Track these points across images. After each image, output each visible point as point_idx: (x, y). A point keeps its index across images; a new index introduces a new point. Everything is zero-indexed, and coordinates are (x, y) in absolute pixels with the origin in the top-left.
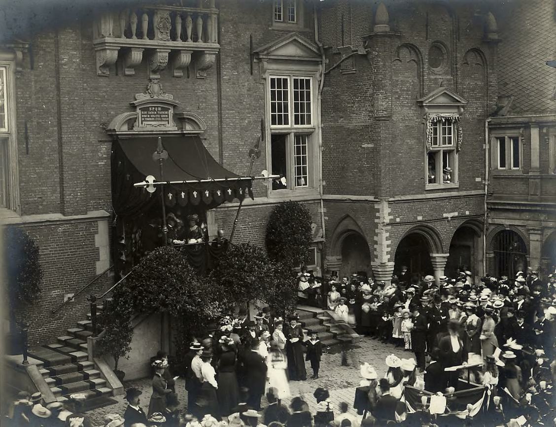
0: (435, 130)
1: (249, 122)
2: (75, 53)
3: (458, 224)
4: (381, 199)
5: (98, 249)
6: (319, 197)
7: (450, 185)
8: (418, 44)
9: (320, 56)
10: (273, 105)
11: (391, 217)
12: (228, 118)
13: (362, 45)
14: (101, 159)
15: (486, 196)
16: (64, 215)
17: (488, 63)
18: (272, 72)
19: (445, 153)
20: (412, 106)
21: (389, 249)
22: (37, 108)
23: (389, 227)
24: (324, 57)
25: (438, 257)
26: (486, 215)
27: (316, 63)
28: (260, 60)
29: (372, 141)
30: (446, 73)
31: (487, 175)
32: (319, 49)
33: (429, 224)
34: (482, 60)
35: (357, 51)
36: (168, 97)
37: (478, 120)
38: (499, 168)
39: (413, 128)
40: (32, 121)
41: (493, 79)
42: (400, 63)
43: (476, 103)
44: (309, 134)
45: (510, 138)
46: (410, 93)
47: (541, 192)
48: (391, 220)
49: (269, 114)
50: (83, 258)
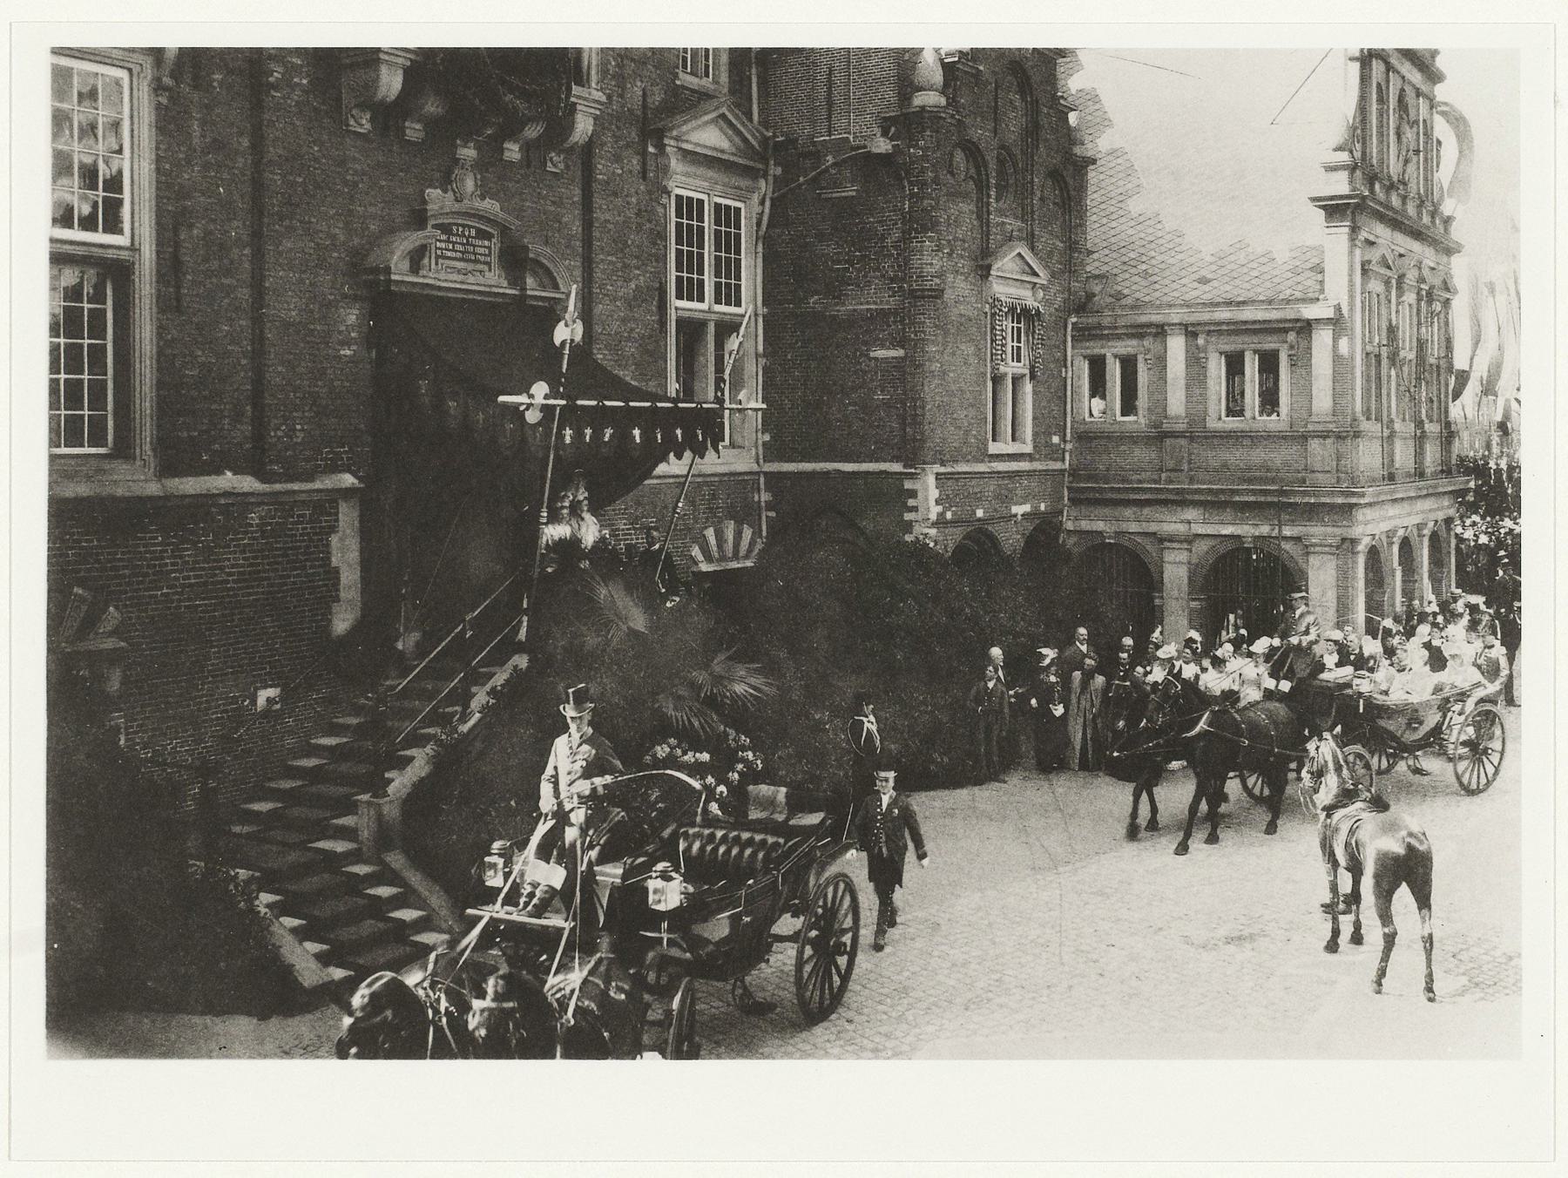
5: (337, 571)
6: (759, 470)
7: (1011, 448)
9: (764, 160)
13: (878, 135)
14: (346, 343)
16: (263, 481)
26: (1065, 514)
29: (901, 344)
35: (865, 147)
36: (490, 206)
38: (1088, 419)
40: (191, 226)
45: (1116, 356)
49: (673, 274)
50: (304, 595)
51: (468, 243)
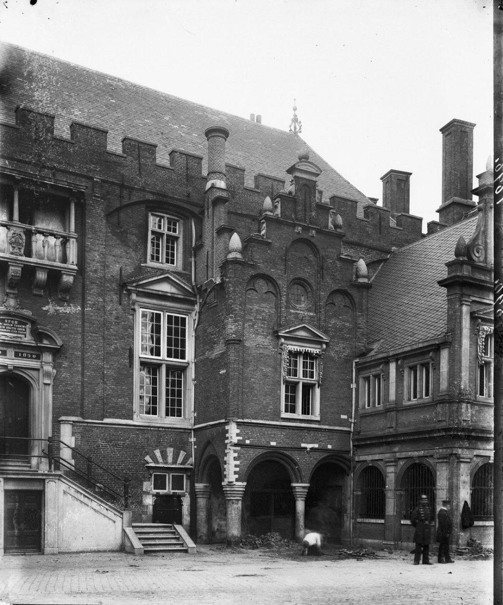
0: (296, 362)
1: (116, 348)
3: (320, 456)
4: (229, 420)
8: (275, 277)
9: (195, 296)
11: (241, 438)
12: (89, 340)
15: (352, 434)
19: (304, 385)
20: (268, 336)
21: (238, 469)
23: (238, 448)
24: (198, 297)
25: (297, 486)
26: (352, 452)
28: (129, 293)
30: (309, 310)
31: (353, 413)
37: (345, 360)
39: (269, 356)
41: (361, 321)
42: (255, 293)
43: (343, 343)
46: (265, 322)
47: (397, 424)
48: (238, 440)
51: (13, 326)
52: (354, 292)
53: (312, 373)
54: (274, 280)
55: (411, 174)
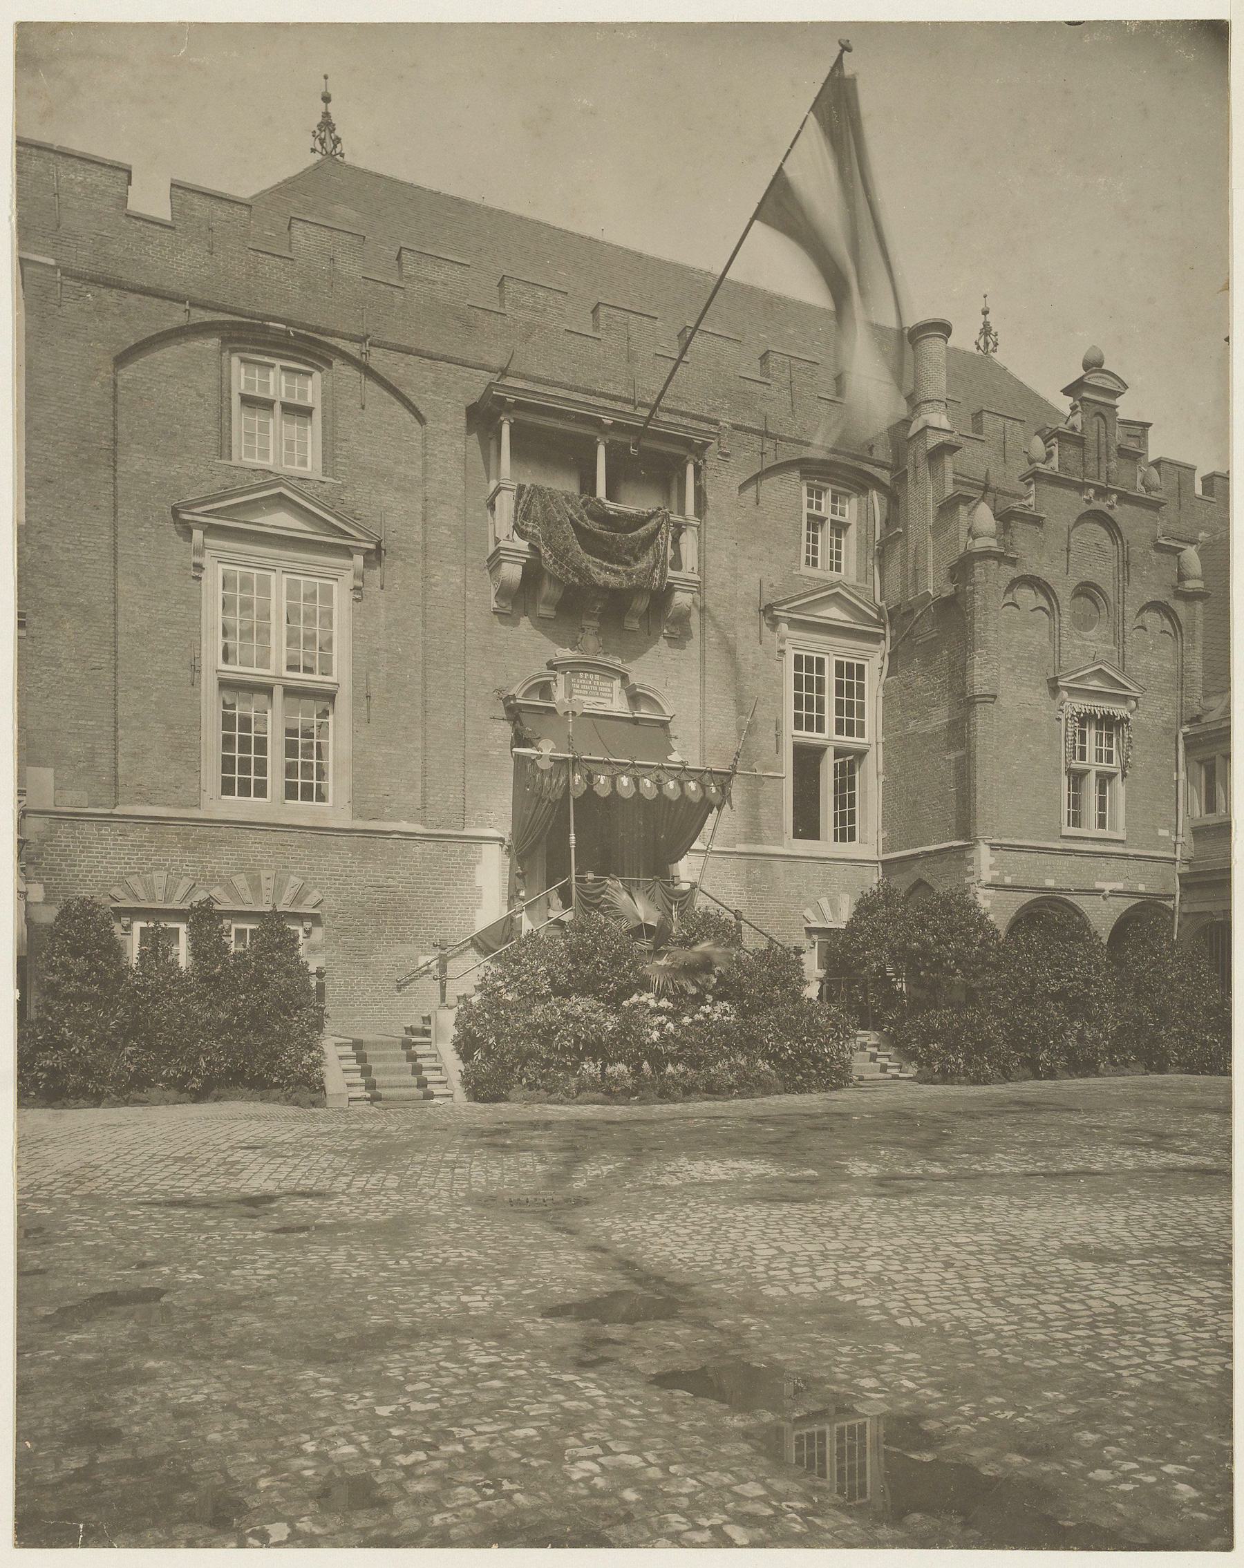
0: (1083, 734)
2: (454, 568)
10: (798, 699)
11: (996, 873)
17: (1184, 631)
18: (796, 643)
19: (1099, 774)
22: (387, 651)
23: (992, 892)
27: (876, 638)
32: (880, 612)
33: (1067, 897)
34: (1173, 626)
44: (861, 755)
48: (993, 877)
51: (593, 684)
52: (1180, 607)
53: (1110, 753)
54: (1049, 586)
55: (1150, 425)
